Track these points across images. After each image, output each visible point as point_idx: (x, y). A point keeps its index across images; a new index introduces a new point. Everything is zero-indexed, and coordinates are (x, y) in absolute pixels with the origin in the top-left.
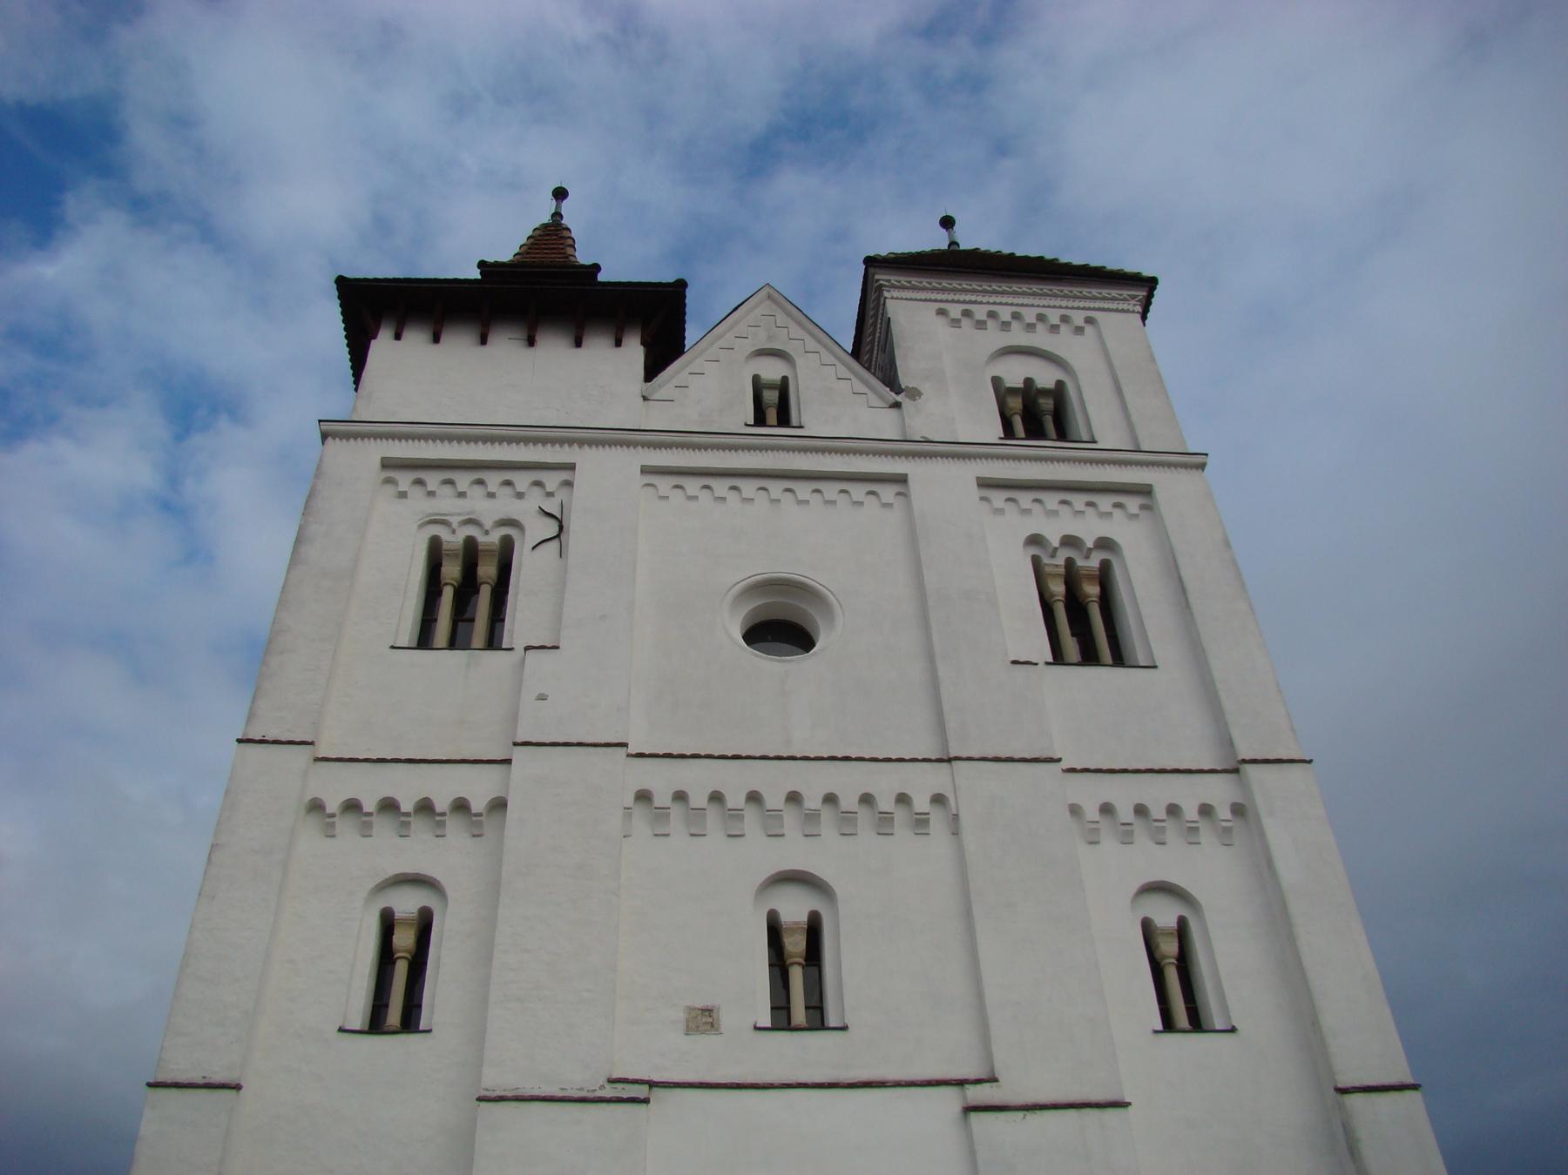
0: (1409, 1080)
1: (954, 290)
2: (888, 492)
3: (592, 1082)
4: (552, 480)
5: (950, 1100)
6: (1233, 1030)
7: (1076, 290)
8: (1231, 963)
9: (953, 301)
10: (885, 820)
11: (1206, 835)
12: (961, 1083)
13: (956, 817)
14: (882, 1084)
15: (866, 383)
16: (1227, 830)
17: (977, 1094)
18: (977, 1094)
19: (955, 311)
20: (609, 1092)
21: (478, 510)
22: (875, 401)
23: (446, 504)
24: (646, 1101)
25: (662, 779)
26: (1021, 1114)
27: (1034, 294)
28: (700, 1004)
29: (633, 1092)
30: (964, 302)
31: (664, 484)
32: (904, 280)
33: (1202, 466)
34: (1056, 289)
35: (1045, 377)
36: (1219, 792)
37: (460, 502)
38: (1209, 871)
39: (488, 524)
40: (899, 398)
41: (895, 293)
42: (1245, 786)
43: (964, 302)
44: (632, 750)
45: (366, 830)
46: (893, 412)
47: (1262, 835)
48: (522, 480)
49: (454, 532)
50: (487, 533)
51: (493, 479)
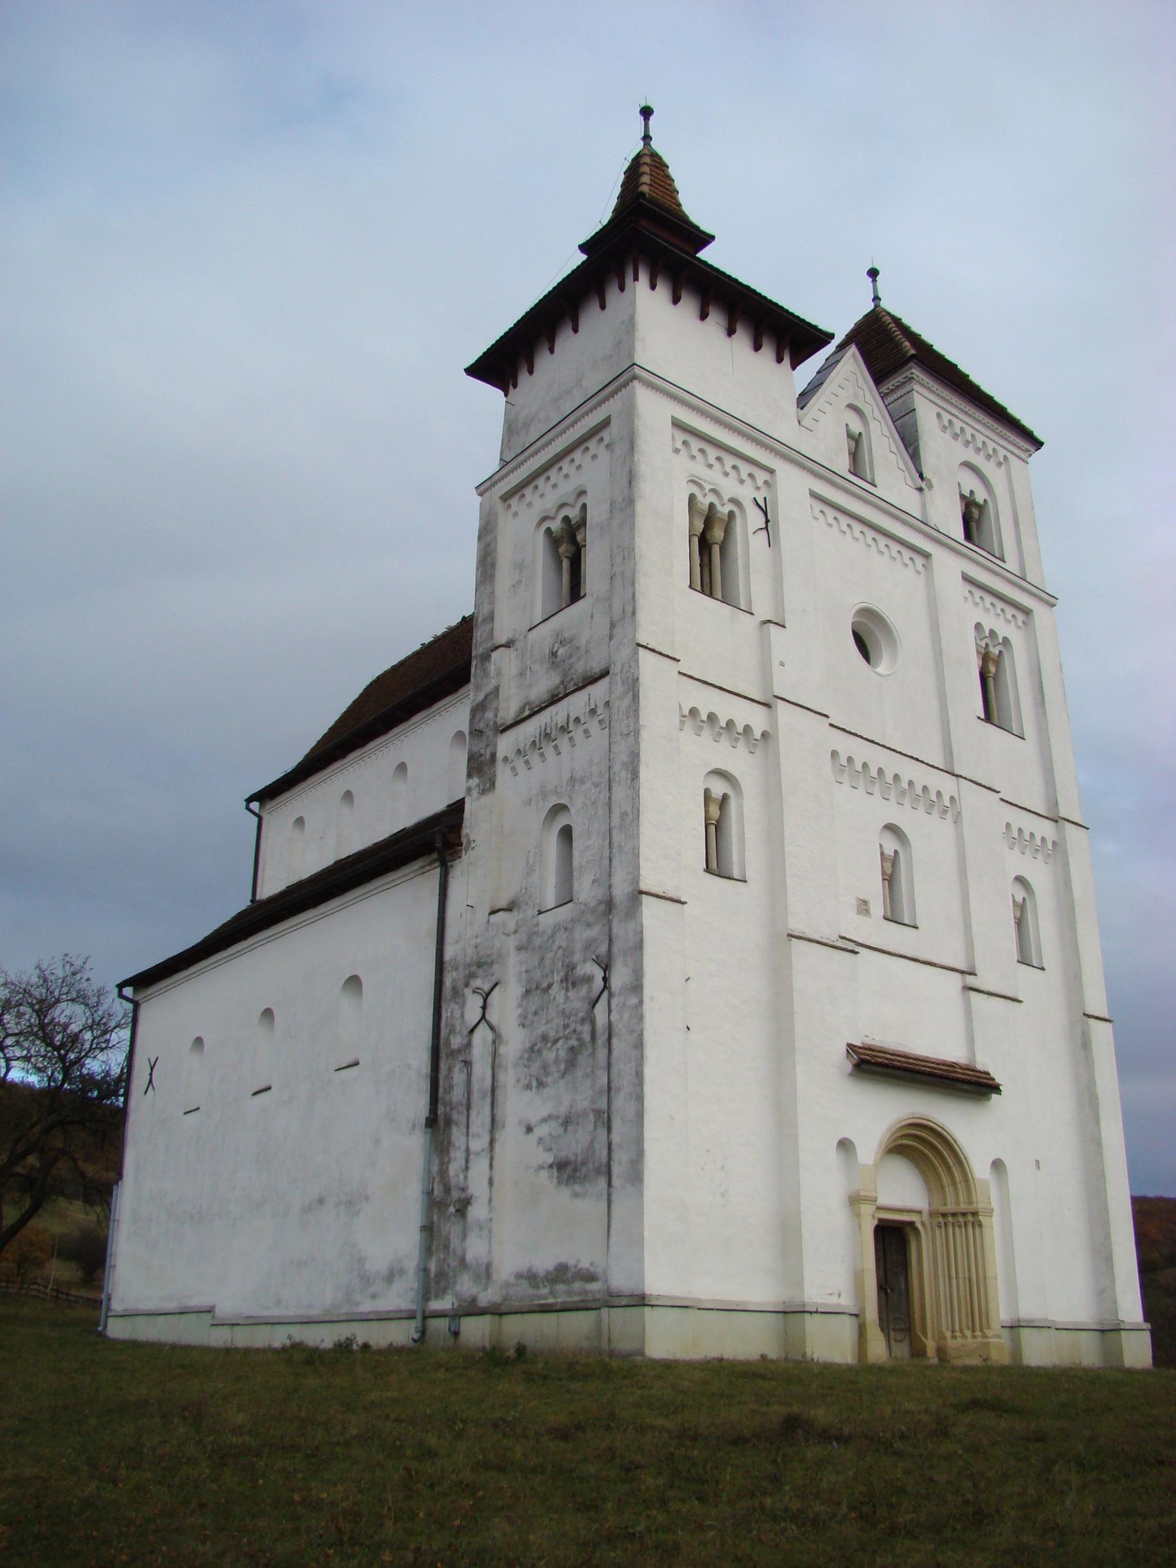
0: (1107, 1017)
3: (832, 938)
4: (761, 476)
5: (956, 980)
6: (1043, 969)
7: (1004, 431)
8: (929, 889)
10: (932, 804)
11: (1040, 856)
12: (962, 972)
13: (959, 813)
15: (906, 464)
17: (971, 981)
18: (971, 981)
19: (946, 417)
20: (840, 943)
21: (731, 487)
24: (856, 953)
27: (984, 425)
29: (849, 947)
30: (953, 415)
31: (818, 506)
32: (934, 385)
33: (1053, 605)
34: (996, 426)
35: (980, 496)
36: (1045, 829)
37: (708, 471)
38: (1040, 875)
39: (726, 499)
40: (923, 485)
42: (1060, 832)
43: (953, 415)
45: (698, 731)
46: (917, 493)
47: (1066, 865)
49: (705, 495)
51: (729, 461)
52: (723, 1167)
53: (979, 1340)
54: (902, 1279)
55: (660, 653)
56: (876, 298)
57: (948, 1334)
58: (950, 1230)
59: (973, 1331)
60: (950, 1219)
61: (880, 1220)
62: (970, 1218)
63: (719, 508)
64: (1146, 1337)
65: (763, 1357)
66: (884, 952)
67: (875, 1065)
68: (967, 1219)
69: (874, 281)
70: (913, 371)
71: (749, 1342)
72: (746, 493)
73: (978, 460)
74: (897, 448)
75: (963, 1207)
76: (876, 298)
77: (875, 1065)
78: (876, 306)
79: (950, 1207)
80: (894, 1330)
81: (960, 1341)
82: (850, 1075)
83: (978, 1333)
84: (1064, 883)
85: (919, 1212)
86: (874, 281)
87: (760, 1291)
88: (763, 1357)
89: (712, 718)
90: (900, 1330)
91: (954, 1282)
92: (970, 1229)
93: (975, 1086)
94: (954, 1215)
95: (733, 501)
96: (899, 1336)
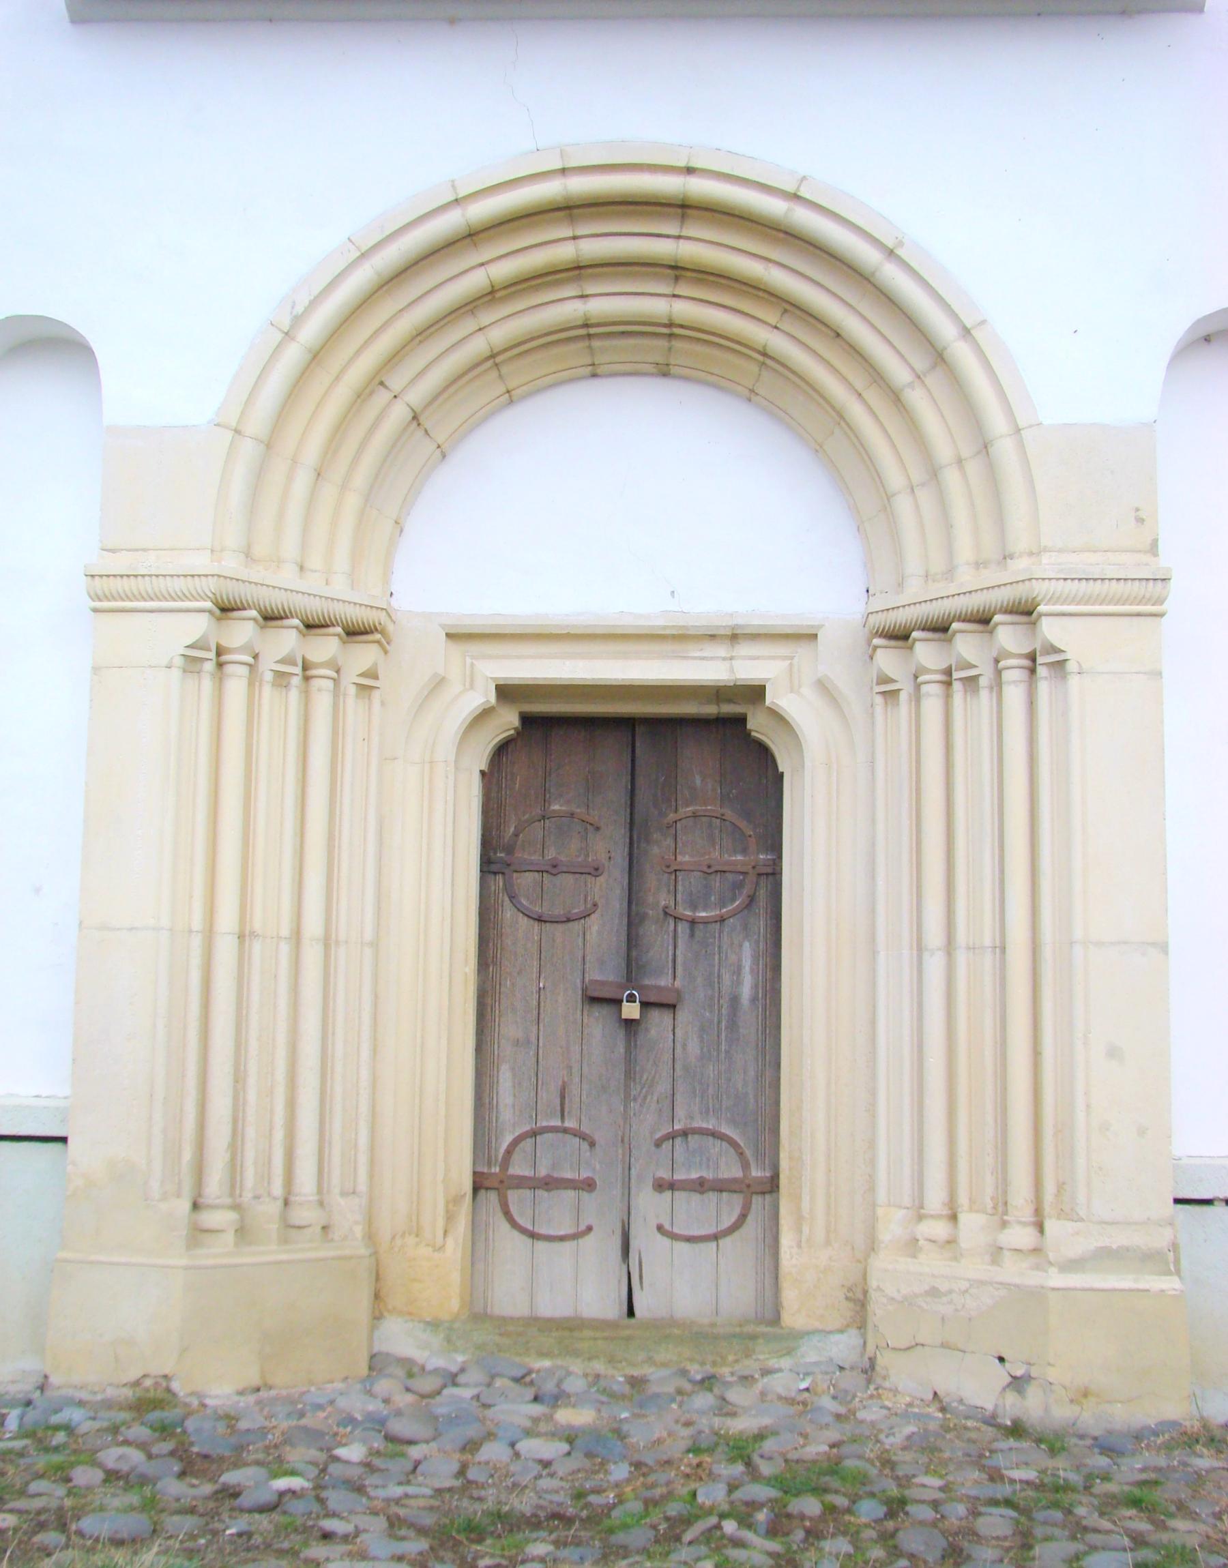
53: (1014, 1271)
57: (892, 1226)
60: (926, 652)
61: (506, 692)
62: (1008, 636)
75: (971, 585)
79: (915, 599)
80: (661, 1186)
81: (931, 1264)
83: (1021, 1236)
91: (935, 966)
92: (1014, 694)
94: (940, 628)
96: (696, 1213)
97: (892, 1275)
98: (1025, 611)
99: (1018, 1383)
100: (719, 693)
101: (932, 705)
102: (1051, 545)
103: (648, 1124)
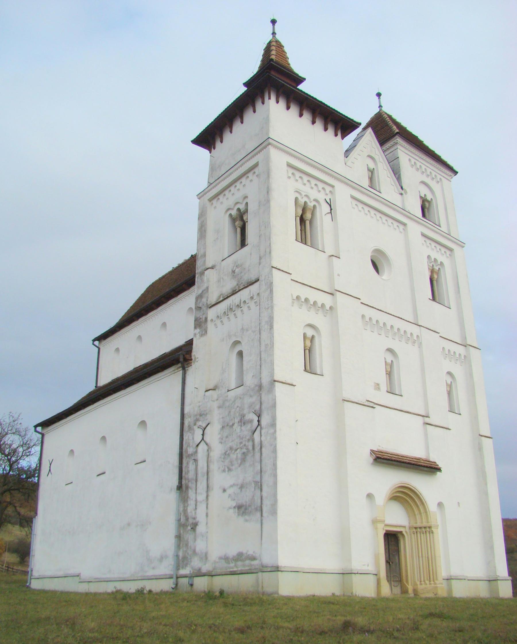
0: (490, 436)
1: (414, 153)
2: (401, 227)
3: (363, 400)
4: (328, 189)
6: (460, 414)
8: (407, 377)
9: (414, 158)
11: (458, 362)
12: (423, 416)
13: (421, 343)
14: (410, 413)
16: (462, 362)
17: (427, 420)
18: (427, 420)
19: (413, 161)
20: (367, 403)
21: (314, 194)
22: (396, 191)
23: (306, 189)
24: (374, 408)
25: (369, 313)
26: (434, 427)
27: (431, 164)
28: (377, 382)
29: (371, 405)
31: (355, 202)
36: (461, 350)
38: (458, 371)
39: (312, 199)
40: (403, 192)
41: (403, 149)
44: (360, 301)
47: (470, 366)
48: (321, 185)
49: (302, 198)
50: (311, 202)
51: (314, 182)
52: (314, 507)
53: (433, 585)
54: (397, 558)
55: (283, 271)
56: (380, 106)
57: (418, 583)
58: (419, 535)
59: (430, 581)
60: (419, 530)
61: (386, 531)
62: (428, 529)
63: (309, 203)
64: (510, 583)
65: (333, 594)
66: (387, 407)
67: (383, 459)
68: (425, 530)
69: (379, 98)
70: (398, 139)
71: (326, 588)
72: (321, 197)
73: (428, 181)
74: (391, 176)
75: (425, 524)
76: (380, 106)
77: (383, 459)
78: (380, 110)
79: (419, 524)
80: (393, 581)
81: (423, 586)
82: (372, 464)
83: (432, 582)
84: (470, 375)
85: (404, 527)
86: (379, 98)
87: (333, 565)
88: (333, 594)
89: (307, 300)
90: (397, 581)
91: (421, 559)
93: (430, 468)
94: (420, 528)
95: (315, 200)
96: (396, 584)
97: (420, 587)
98: (430, 527)
99: (435, 595)
100: (395, 531)
101: (419, 535)
102: (432, 523)
103: (392, 575)
